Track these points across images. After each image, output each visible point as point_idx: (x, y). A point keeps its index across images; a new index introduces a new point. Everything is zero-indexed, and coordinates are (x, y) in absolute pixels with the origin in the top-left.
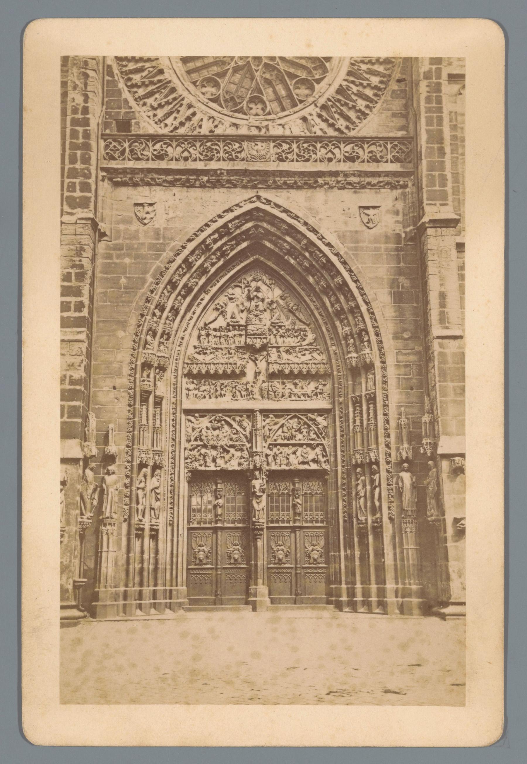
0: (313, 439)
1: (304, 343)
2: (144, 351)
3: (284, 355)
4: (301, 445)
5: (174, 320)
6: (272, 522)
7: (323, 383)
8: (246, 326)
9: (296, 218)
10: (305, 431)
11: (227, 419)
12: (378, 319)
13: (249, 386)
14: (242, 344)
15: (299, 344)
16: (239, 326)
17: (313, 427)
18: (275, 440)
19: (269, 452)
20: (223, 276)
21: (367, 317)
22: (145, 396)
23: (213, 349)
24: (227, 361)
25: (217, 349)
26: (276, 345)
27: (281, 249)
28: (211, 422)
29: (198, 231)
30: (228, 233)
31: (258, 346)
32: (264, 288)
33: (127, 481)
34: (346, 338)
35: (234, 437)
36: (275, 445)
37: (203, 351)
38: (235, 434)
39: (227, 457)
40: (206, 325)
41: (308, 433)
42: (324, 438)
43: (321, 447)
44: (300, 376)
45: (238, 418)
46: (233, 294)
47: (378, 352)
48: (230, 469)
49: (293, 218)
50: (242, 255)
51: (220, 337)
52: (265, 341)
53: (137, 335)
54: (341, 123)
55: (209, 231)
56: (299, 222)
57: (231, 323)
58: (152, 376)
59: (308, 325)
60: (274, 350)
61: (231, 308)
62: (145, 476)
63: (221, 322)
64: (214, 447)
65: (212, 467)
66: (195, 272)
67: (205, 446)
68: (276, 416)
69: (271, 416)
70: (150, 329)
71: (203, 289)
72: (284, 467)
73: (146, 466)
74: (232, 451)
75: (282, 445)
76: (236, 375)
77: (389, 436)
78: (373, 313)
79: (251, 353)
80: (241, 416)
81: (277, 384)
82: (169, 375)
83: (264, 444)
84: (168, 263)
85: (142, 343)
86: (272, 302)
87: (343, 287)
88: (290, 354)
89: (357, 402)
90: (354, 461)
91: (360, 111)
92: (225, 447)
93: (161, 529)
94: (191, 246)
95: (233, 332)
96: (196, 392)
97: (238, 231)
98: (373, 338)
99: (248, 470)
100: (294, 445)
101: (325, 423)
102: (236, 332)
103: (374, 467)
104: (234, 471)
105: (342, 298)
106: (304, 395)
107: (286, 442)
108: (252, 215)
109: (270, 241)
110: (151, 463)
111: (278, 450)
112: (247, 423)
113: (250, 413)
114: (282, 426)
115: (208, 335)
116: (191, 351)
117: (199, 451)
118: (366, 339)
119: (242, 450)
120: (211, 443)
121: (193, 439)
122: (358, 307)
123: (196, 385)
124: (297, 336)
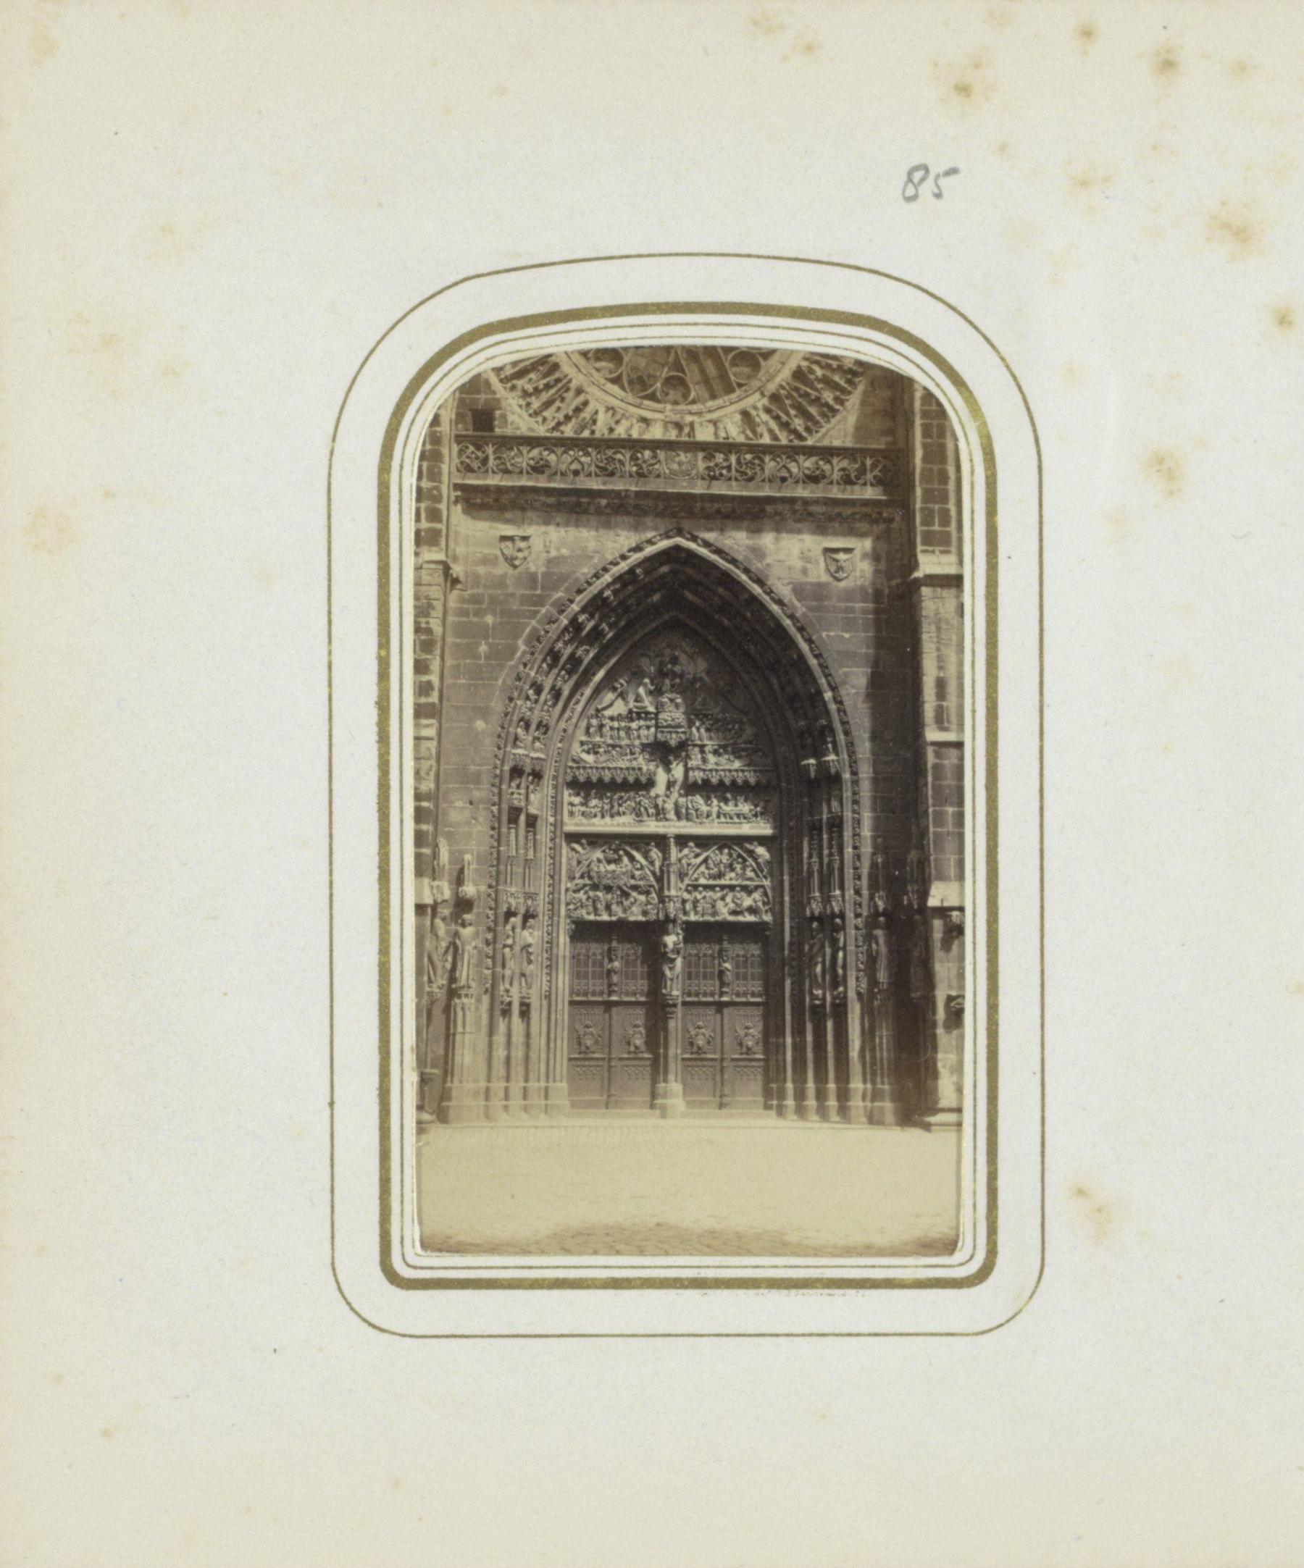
0: (750, 879)
4: (732, 888)
6: (689, 995)
9: (733, 561)
13: (660, 801)
14: (651, 739)
17: (750, 861)
18: (696, 880)
19: (686, 896)
22: (514, 814)
25: (614, 746)
31: (673, 743)
32: (683, 658)
33: (490, 936)
35: (637, 873)
36: (696, 887)
39: (626, 903)
40: (598, 711)
41: (744, 869)
48: (632, 919)
51: (618, 729)
52: (683, 737)
53: (503, 728)
54: (798, 424)
58: (523, 785)
59: (746, 714)
62: (513, 929)
64: (608, 889)
67: (595, 887)
70: (522, 719)
73: (514, 914)
74: (634, 894)
75: (706, 887)
77: (859, 878)
78: (841, 703)
82: (547, 782)
85: (511, 738)
86: (695, 680)
88: (720, 755)
90: (808, 913)
91: (827, 405)
93: (535, 1003)
96: (583, 809)
98: (841, 737)
99: (657, 922)
100: (723, 887)
102: (642, 723)
103: (838, 921)
104: (637, 923)
106: (738, 816)
107: (711, 882)
109: (696, 593)
110: (522, 911)
112: (655, 854)
113: (660, 841)
114: (705, 861)
120: (605, 882)
121: (577, 875)
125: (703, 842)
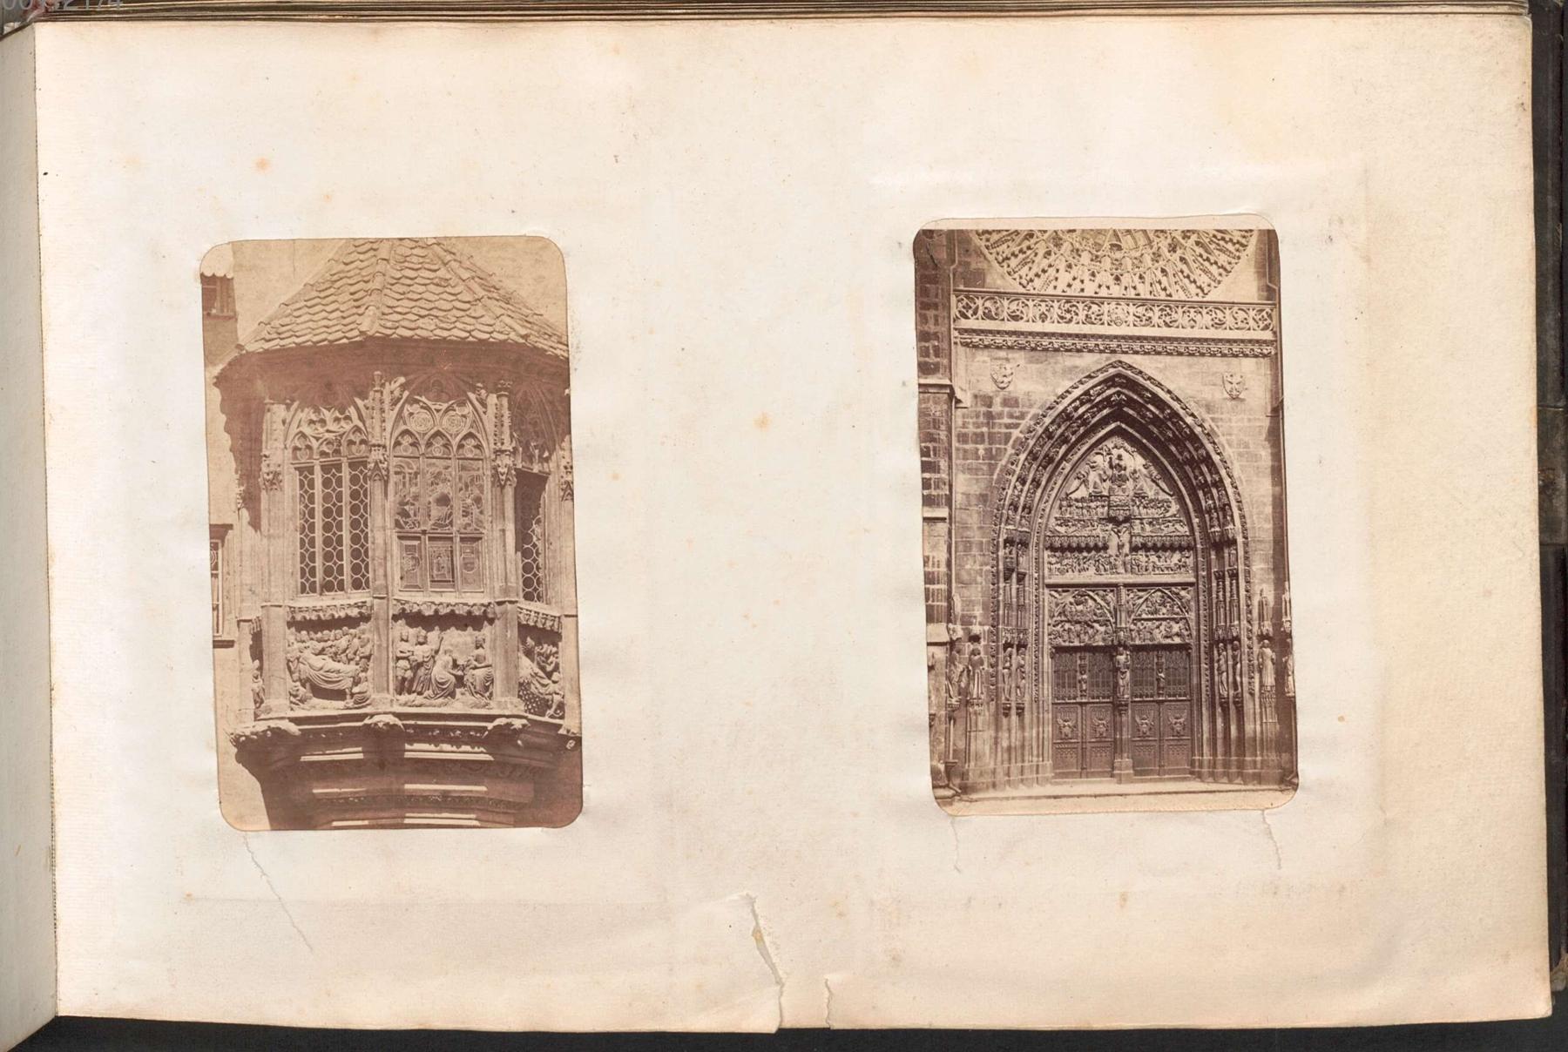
9: (1159, 385)
21: (1230, 491)
30: (1089, 401)
32: (1125, 455)
34: (1209, 512)
37: (1065, 522)
39: (1091, 631)
44: (1164, 548)
50: (1104, 421)
61: (1093, 477)
63: (1082, 492)
65: (1077, 643)
71: (1064, 458)
81: (1141, 557)
82: (1032, 552)
86: (1135, 472)
87: (1208, 460)
89: (1220, 578)
93: (1027, 706)
105: (1205, 469)
116: (1052, 522)
122: (1221, 480)
125: (1144, 587)
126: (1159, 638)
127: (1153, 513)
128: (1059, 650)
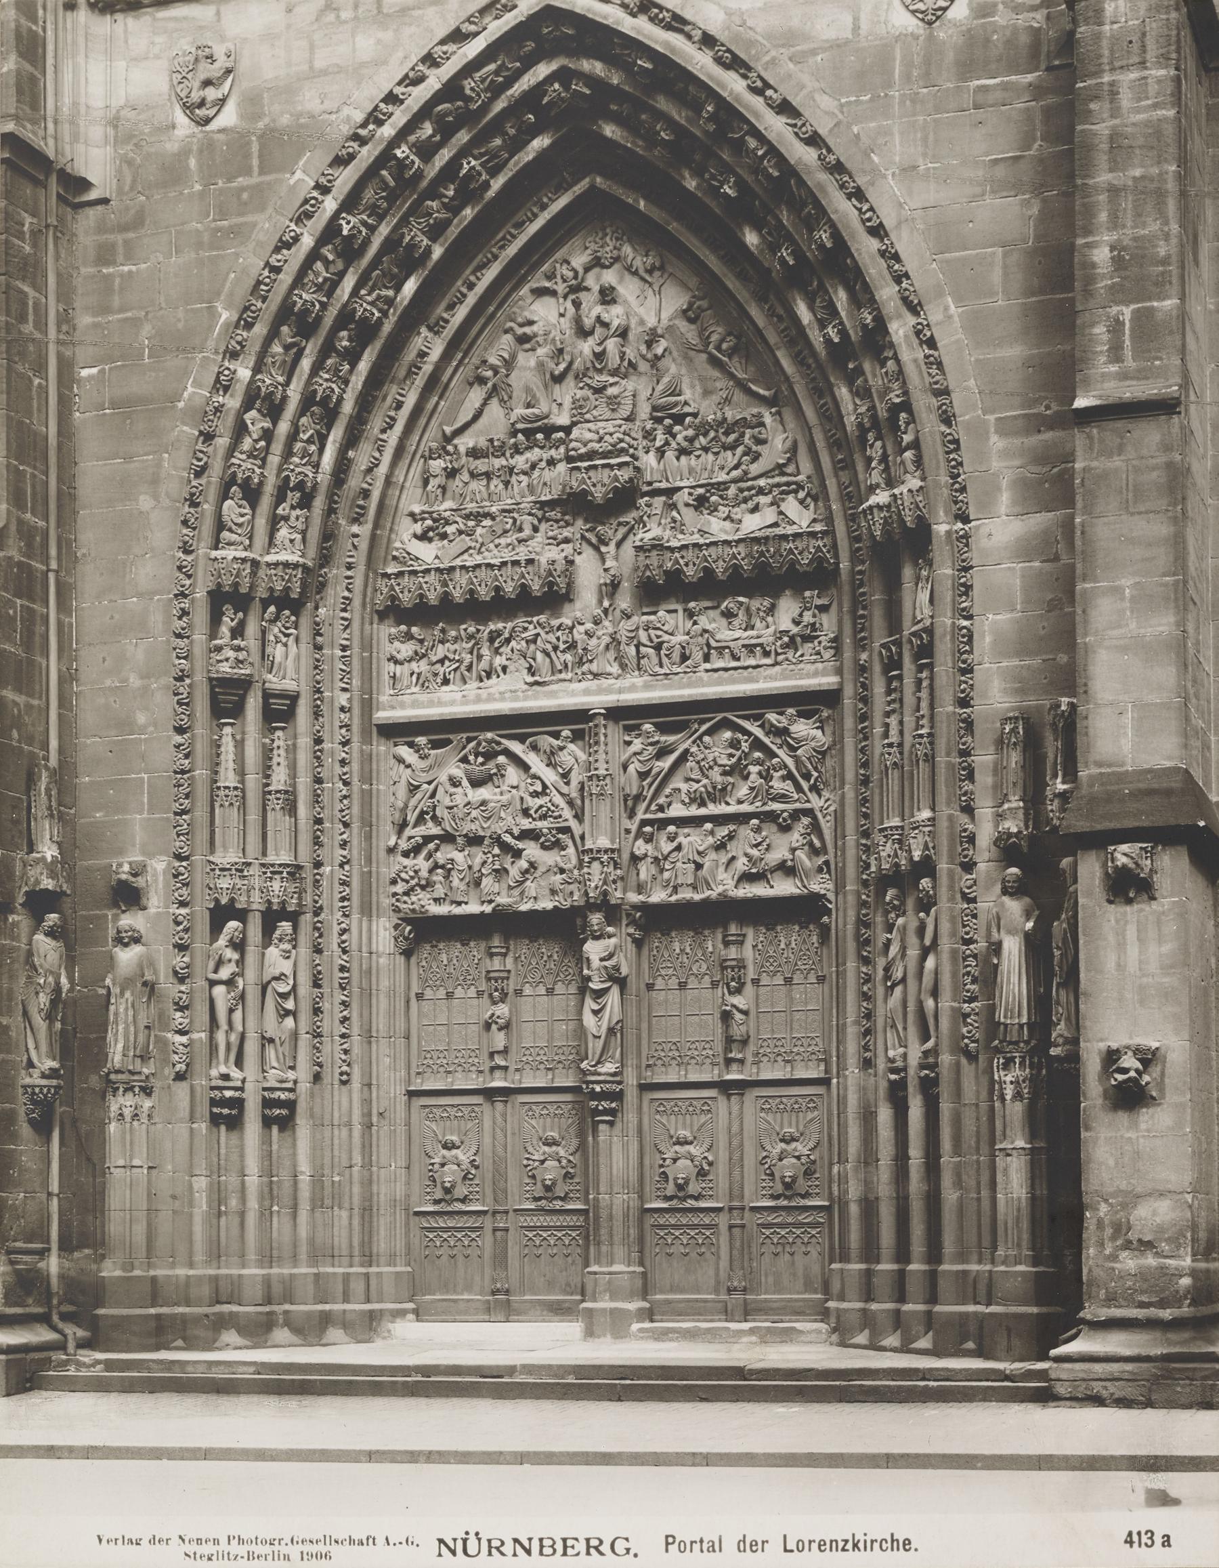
0: (781, 798)
1: (755, 469)
2: (214, 554)
3: (688, 515)
5: (322, 440)
7: (819, 602)
8: (567, 430)
10: (754, 769)
11: (516, 747)
12: (946, 361)
15: (735, 473)
16: (549, 430)
20: (483, 266)
23: (467, 517)
24: (507, 556)
25: (479, 516)
26: (664, 485)
27: (652, 140)
28: (464, 760)
29: (364, 125)
30: (466, 118)
31: (599, 494)
32: (628, 289)
35: (533, 803)
38: (535, 794)
42: (814, 788)
43: (806, 821)
45: (547, 741)
46: (531, 323)
47: (945, 479)
48: (524, 907)
49: (669, 27)
52: (625, 475)
55: (400, 117)
56: (689, 37)
57: (520, 426)
58: (252, 629)
60: (659, 501)
63: (496, 421)
64: (474, 840)
65: (473, 908)
66: (376, 262)
67: (448, 838)
68: (663, 729)
69: (648, 727)
72: (686, 894)
74: (531, 850)
76: (554, 597)
78: (931, 343)
79: (586, 521)
80: (556, 735)
81: (672, 621)
83: (627, 824)
84: (277, 250)
88: (713, 510)
92: (508, 838)
94: (345, 178)
95: (528, 455)
97: (500, 105)
100: (719, 820)
101: (820, 738)
105: (841, 298)
106: (750, 649)
107: (694, 811)
108: (538, 38)
111: (671, 839)
113: (577, 722)
115: (452, 473)
117: (429, 856)
118: (907, 438)
119: (558, 845)
120: (468, 827)
121: (412, 818)
123: (421, 641)
124: (732, 447)
126: (725, 884)
127: (714, 466)
128: (423, 932)
